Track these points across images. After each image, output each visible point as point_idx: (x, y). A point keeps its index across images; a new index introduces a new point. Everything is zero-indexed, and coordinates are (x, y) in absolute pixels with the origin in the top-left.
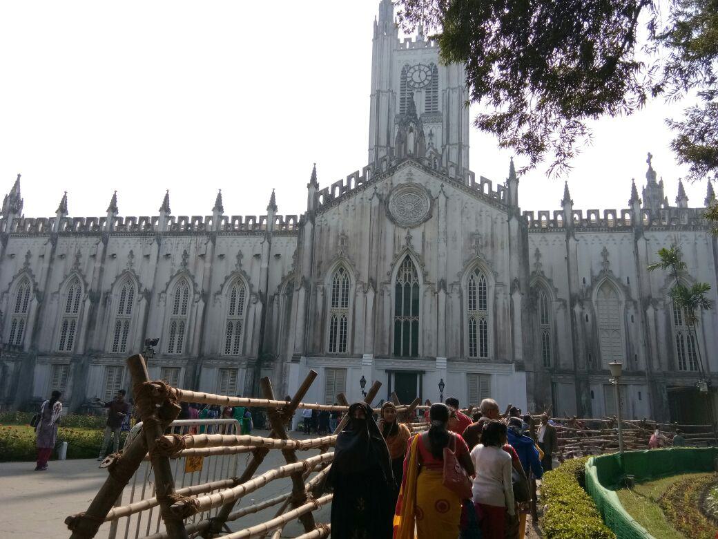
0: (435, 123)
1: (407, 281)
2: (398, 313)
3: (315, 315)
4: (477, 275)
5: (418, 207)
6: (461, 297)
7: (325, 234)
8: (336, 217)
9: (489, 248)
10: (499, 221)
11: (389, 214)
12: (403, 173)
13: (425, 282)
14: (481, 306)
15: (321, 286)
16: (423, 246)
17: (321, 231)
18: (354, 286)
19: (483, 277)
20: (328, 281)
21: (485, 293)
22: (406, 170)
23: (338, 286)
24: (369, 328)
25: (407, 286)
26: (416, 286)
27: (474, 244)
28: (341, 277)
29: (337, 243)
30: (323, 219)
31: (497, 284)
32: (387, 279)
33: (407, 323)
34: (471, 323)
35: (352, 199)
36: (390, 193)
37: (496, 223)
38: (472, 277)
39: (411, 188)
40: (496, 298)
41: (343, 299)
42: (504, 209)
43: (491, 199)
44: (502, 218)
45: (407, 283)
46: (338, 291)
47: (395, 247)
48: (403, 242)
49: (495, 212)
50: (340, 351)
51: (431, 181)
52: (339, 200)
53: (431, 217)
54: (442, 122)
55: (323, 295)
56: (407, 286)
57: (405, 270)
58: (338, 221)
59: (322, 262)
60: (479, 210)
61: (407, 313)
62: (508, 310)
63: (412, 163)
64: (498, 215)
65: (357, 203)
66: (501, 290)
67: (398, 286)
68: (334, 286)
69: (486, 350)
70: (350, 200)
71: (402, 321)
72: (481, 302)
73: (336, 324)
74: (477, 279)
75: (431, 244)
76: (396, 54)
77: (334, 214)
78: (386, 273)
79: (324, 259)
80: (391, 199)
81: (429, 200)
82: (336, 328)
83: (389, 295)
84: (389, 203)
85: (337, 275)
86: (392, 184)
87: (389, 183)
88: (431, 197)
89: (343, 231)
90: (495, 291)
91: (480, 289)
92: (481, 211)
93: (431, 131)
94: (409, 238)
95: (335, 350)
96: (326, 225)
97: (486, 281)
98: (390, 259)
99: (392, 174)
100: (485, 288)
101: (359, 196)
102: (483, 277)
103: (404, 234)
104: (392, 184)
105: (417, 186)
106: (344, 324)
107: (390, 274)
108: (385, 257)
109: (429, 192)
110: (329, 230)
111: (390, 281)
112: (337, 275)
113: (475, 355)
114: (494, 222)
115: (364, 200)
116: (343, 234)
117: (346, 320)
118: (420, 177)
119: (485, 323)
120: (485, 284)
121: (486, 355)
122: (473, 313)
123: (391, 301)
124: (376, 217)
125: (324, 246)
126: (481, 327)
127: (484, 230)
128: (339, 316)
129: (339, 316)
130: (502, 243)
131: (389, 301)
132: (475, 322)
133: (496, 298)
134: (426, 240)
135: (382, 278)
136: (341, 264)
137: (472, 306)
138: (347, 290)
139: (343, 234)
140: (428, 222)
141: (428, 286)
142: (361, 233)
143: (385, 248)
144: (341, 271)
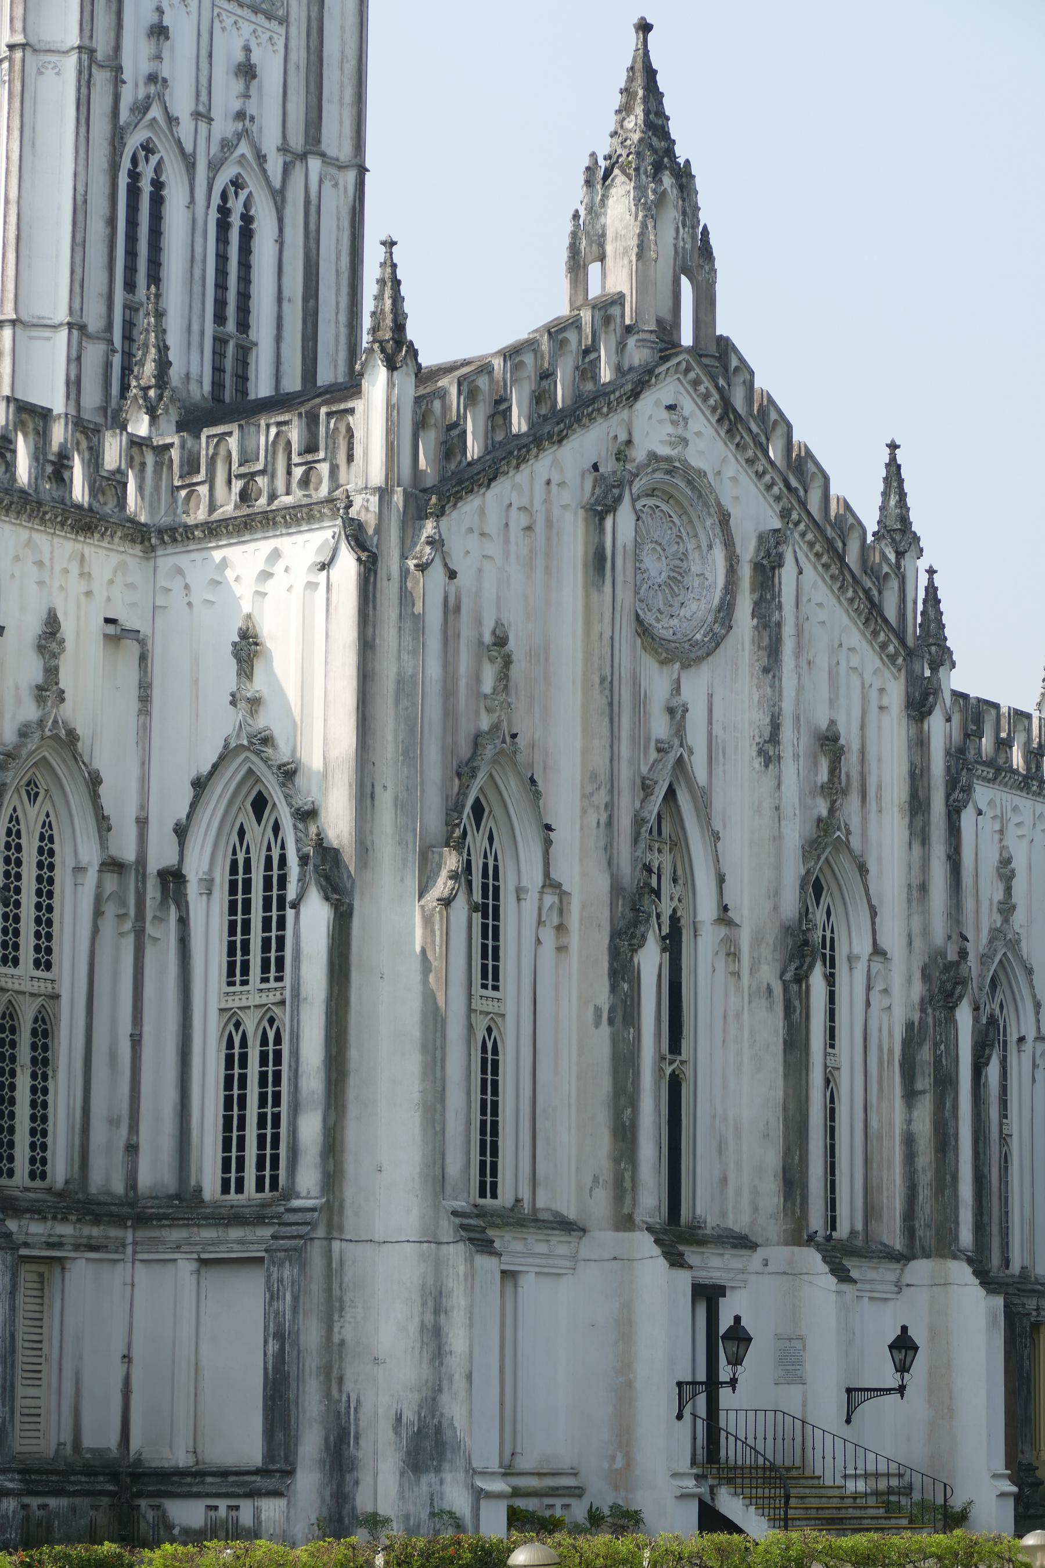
0: (260, 19)
27: (823, 776)
29: (478, 681)
31: (878, 951)
35: (522, 476)
44: (882, 690)
48: (660, 727)
54: (284, 21)
58: (480, 571)
62: (891, 1051)
65: (538, 506)
81: (719, 555)
88: (729, 544)
89: (499, 623)
93: (247, 50)
101: (543, 465)
103: (658, 684)
109: (724, 519)
118: (707, 448)
141: (723, 931)
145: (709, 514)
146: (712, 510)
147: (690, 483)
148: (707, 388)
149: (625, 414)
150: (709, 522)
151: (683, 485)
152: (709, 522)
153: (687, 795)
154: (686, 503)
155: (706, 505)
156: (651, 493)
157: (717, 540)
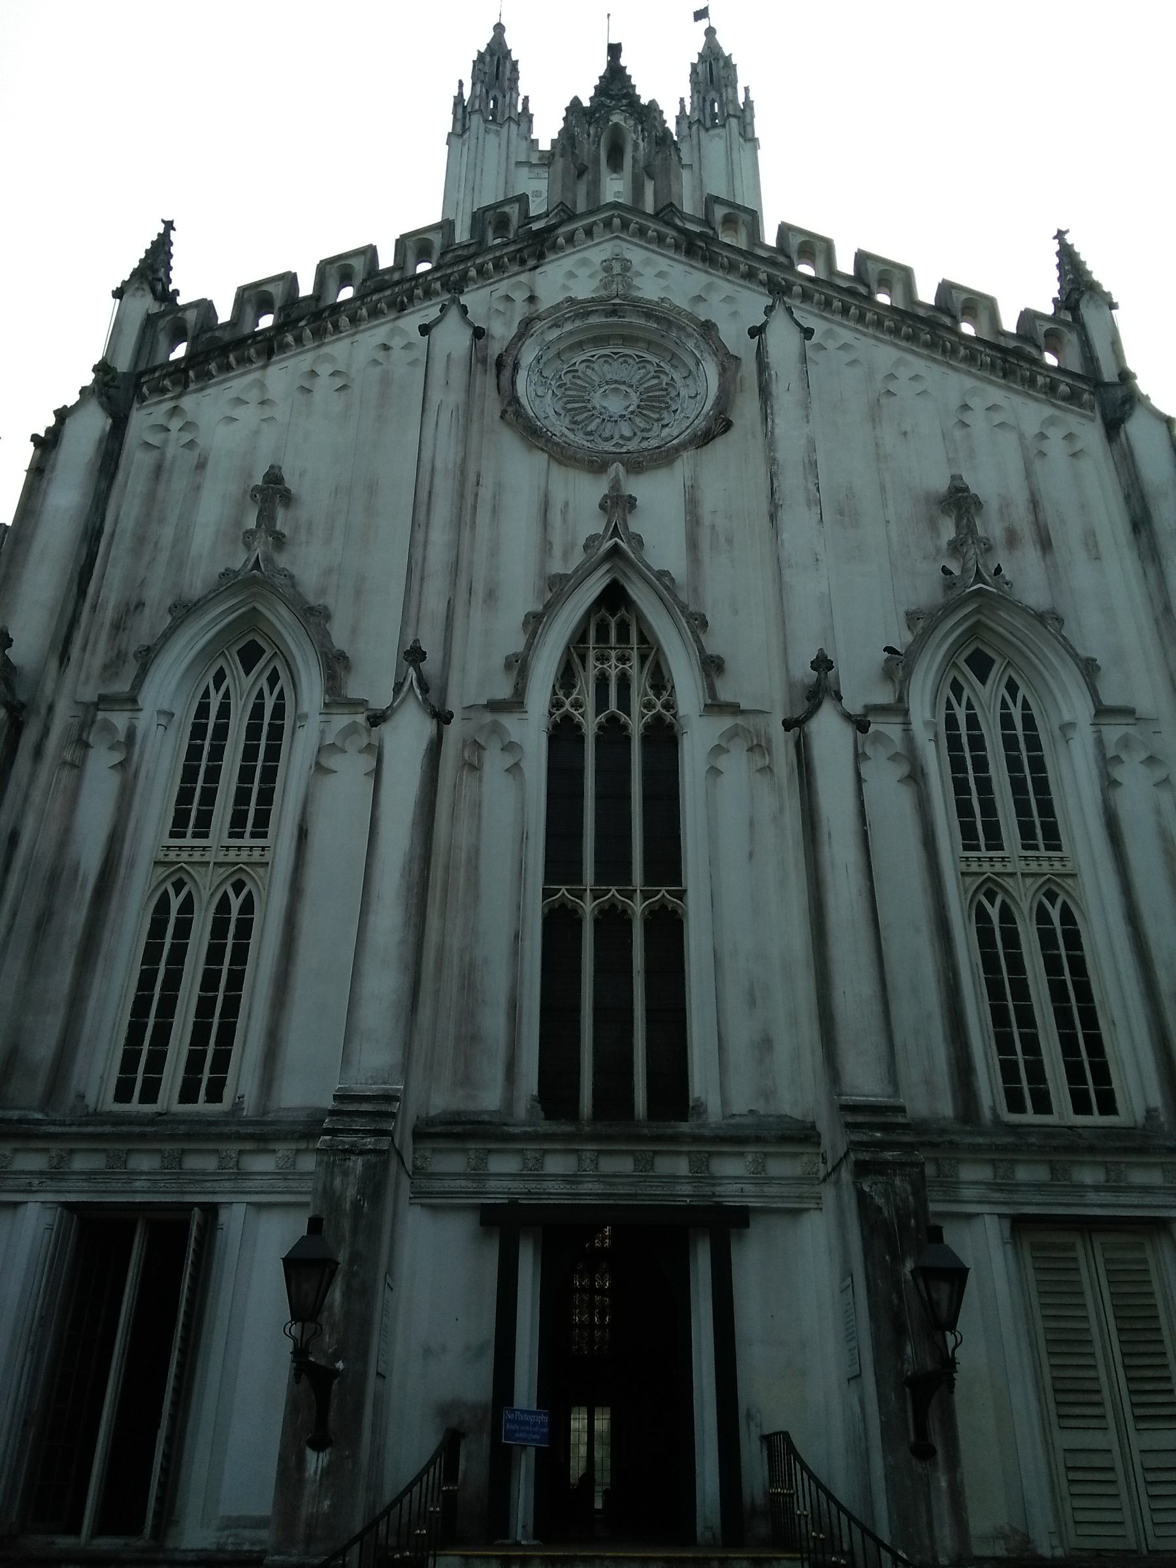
1: (613, 706)
2: (561, 862)
3: (53, 879)
4: (983, 681)
5: (656, 402)
6: (916, 777)
7: (179, 484)
8: (248, 415)
9: (1030, 554)
10: (1056, 446)
11: (514, 413)
12: (585, 262)
13: (715, 706)
14: (1026, 831)
15: (119, 720)
16: (693, 545)
17: (158, 470)
18: (314, 722)
19: (1012, 687)
20: (168, 688)
21: (1038, 765)
22: (598, 253)
23: (221, 732)
24: (389, 919)
25: (613, 734)
26: (664, 738)
28: (244, 688)
30: (175, 424)
31: (1102, 712)
32: (503, 690)
33: (613, 922)
34: (982, 916)
36: (526, 325)
37: (1042, 454)
38: (957, 688)
39: (618, 323)
40: (1109, 783)
41: (242, 796)
42: (1073, 397)
43: (1010, 358)
44: (1069, 437)
45: (613, 719)
46: (217, 753)
47: (546, 546)
49: (1030, 413)
50: (188, 1094)
51: (715, 298)
52: (268, 347)
53: (728, 426)
55: (122, 765)
56: (613, 734)
57: (602, 658)
58: (257, 433)
59: (141, 605)
60: (954, 402)
61: (613, 866)
63: (625, 225)
64: (1051, 421)
66: (1125, 742)
67: (563, 735)
68: (198, 731)
69: (1102, 1073)
70: (325, 350)
71: (588, 907)
72: (1022, 808)
73: (183, 929)
74: (987, 697)
75: (729, 541)
76: (524, 171)
77: (239, 401)
78: (499, 661)
79: (157, 594)
80: (528, 355)
82: (178, 954)
83: (515, 769)
84: (516, 367)
85: (220, 677)
86: (532, 299)
87: (520, 296)
90: (1100, 743)
91: (1010, 743)
92: (965, 407)
94: (618, 504)
95: (150, 1094)
96: (191, 444)
97: (1035, 712)
98: (520, 595)
99: (531, 263)
100: (1034, 743)
101: (374, 335)
102: (1012, 687)
104: (532, 299)
105: (649, 311)
106: (234, 930)
107: (519, 666)
108: (491, 595)
109: (708, 328)
110: (201, 465)
111: (520, 691)
112: (220, 677)
113: (1043, 1104)
114: (1033, 455)
115: (396, 352)
116: (274, 478)
117: (248, 906)
118: (663, 279)
119: (1067, 916)
120: (1029, 722)
121: (1108, 1105)
122: (985, 862)
123: (522, 807)
124: (455, 397)
125: (167, 533)
126: (1047, 939)
127: (995, 479)
128: (207, 889)
129: (207, 889)
130: (1091, 541)
131: (509, 806)
132: (1006, 915)
133: (1109, 783)
134: (707, 519)
135: (474, 678)
136: (251, 619)
137: (979, 830)
138: (273, 753)
139: (274, 478)
140: (719, 443)
141: (726, 722)
142: (372, 489)
143: (494, 553)
144: (250, 657)
145: (689, 336)
146: (689, 330)
147: (649, 315)
148: (655, 230)
149: (524, 278)
150: (690, 344)
151: (642, 321)
152: (690, 344)
153: (640, 584)
154: (655, 338)
155: (682, 328)
156: (599, 340)
157: (706, 355)
